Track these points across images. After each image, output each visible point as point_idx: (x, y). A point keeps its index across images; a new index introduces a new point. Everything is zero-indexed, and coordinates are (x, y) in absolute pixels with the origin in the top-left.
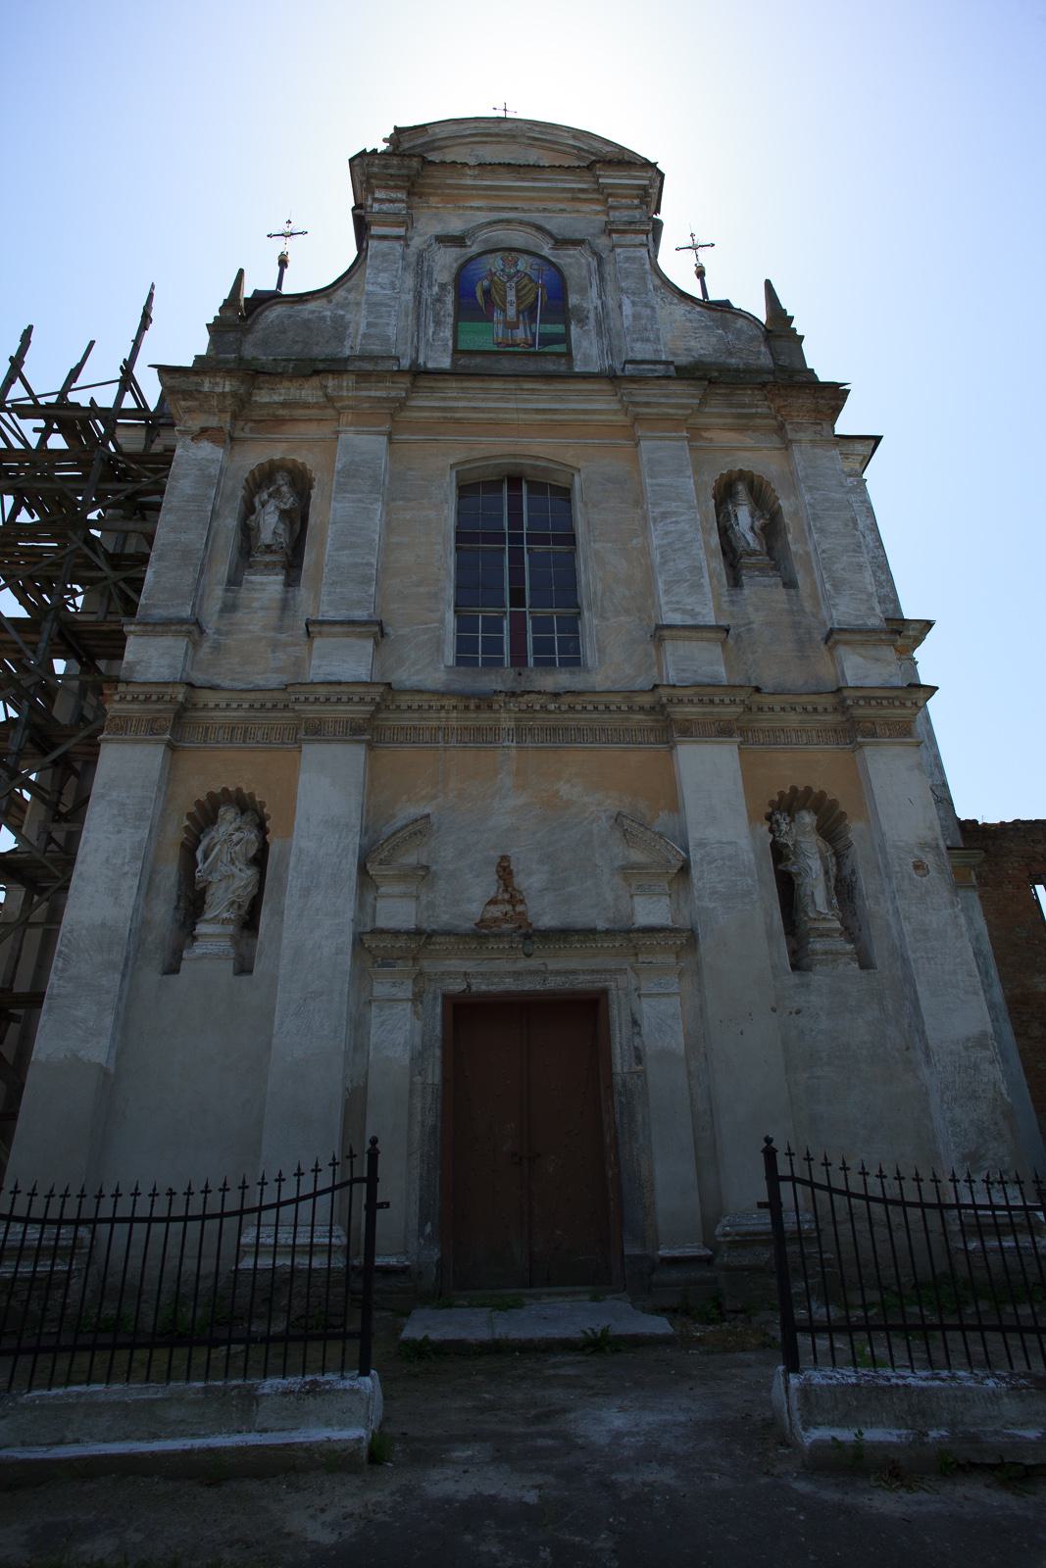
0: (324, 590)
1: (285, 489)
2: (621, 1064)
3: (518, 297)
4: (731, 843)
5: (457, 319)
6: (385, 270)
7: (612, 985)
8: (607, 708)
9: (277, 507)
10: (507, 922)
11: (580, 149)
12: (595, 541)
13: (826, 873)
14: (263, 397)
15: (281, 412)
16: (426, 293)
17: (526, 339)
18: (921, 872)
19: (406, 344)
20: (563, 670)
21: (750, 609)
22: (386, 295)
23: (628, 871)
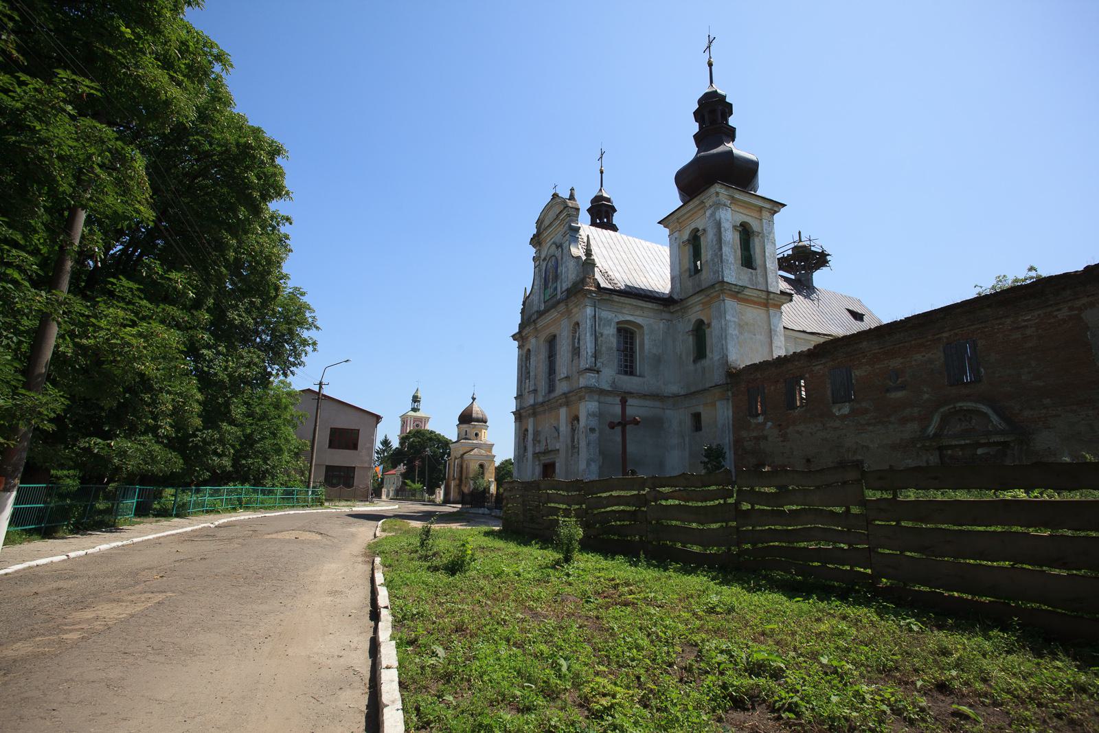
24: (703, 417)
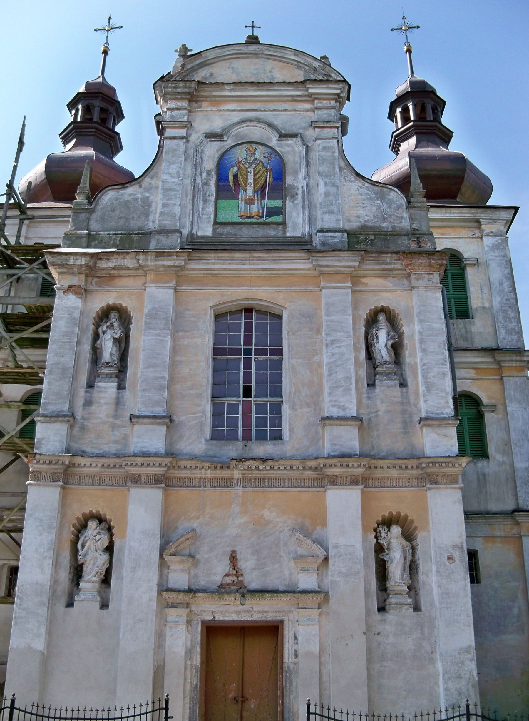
0: (139, 394)
1: (116, 324)
2: (288, 657)
3: (255, 180)
4: (351, 546)
5: (217, 199)
6: (173, 163)
7: (285, 618)
8: (291, 467)
9: (112, 336)
10: (234, 585)
11: (298, 62)
12: (292, 358)
13: (405, 558)
14: (103, 264)
15: (113, 272)
16: (198, 179)
17: (258, 212)
18: (451, 561)
19: (186, 217)
20: (270, 442)
21: (378, 402)
22: (173, 182)
23: (298, 558)
24: (483, 560)
